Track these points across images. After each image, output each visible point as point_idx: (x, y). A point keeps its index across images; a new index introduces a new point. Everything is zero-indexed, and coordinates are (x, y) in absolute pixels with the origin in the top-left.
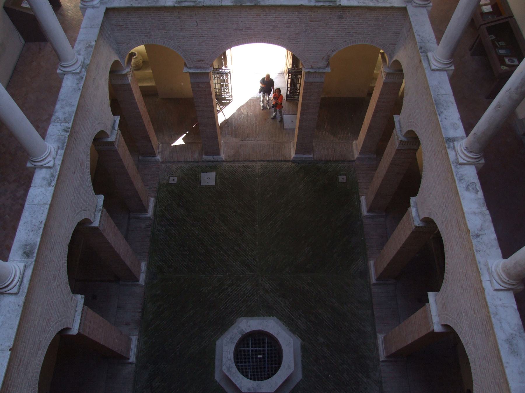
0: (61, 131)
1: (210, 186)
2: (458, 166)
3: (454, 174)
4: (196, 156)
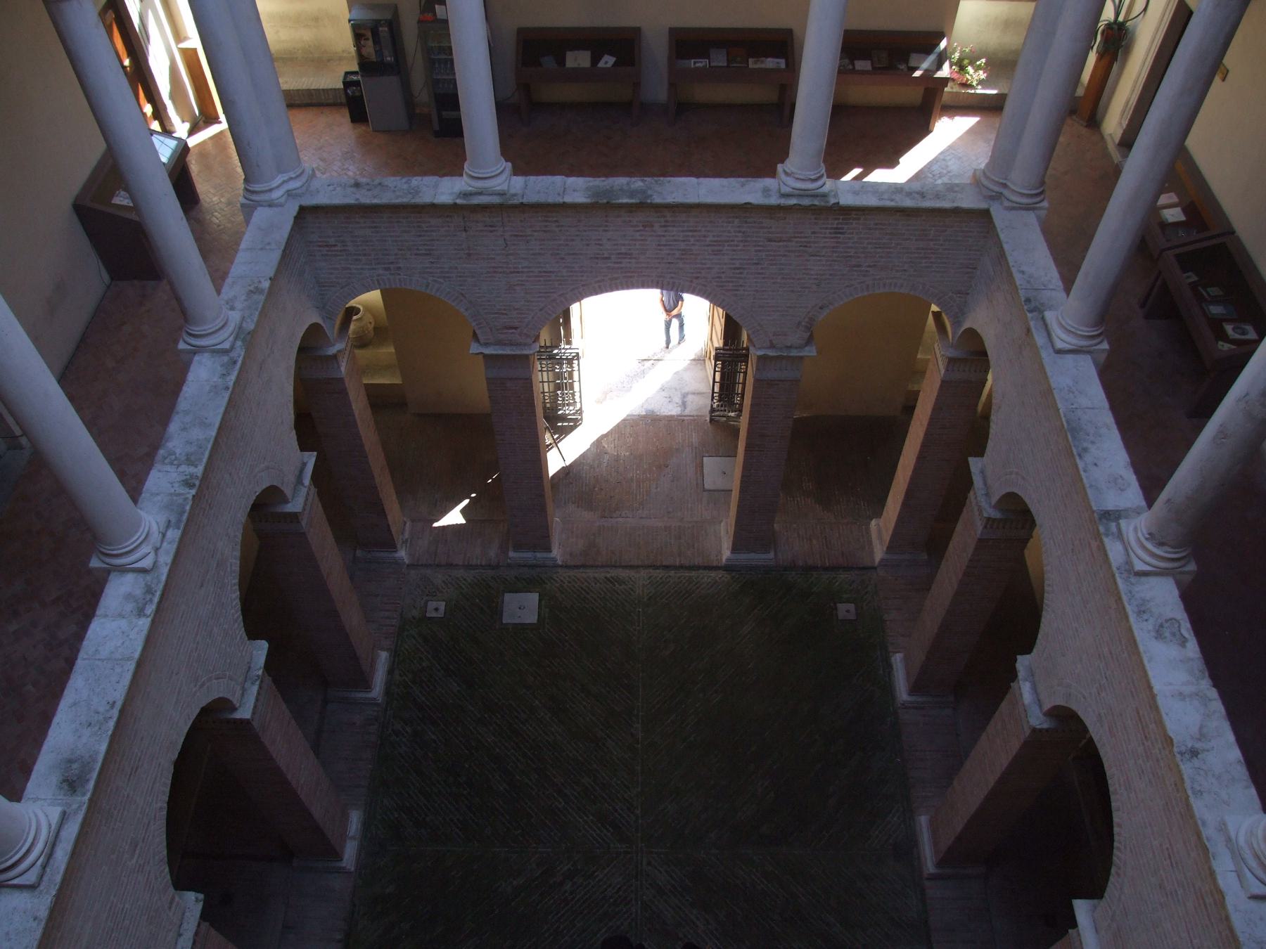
0: (176, 485)
1: (521, 628)
2: (1133, 580)
3: (1124, 598)
4: (493, 553)
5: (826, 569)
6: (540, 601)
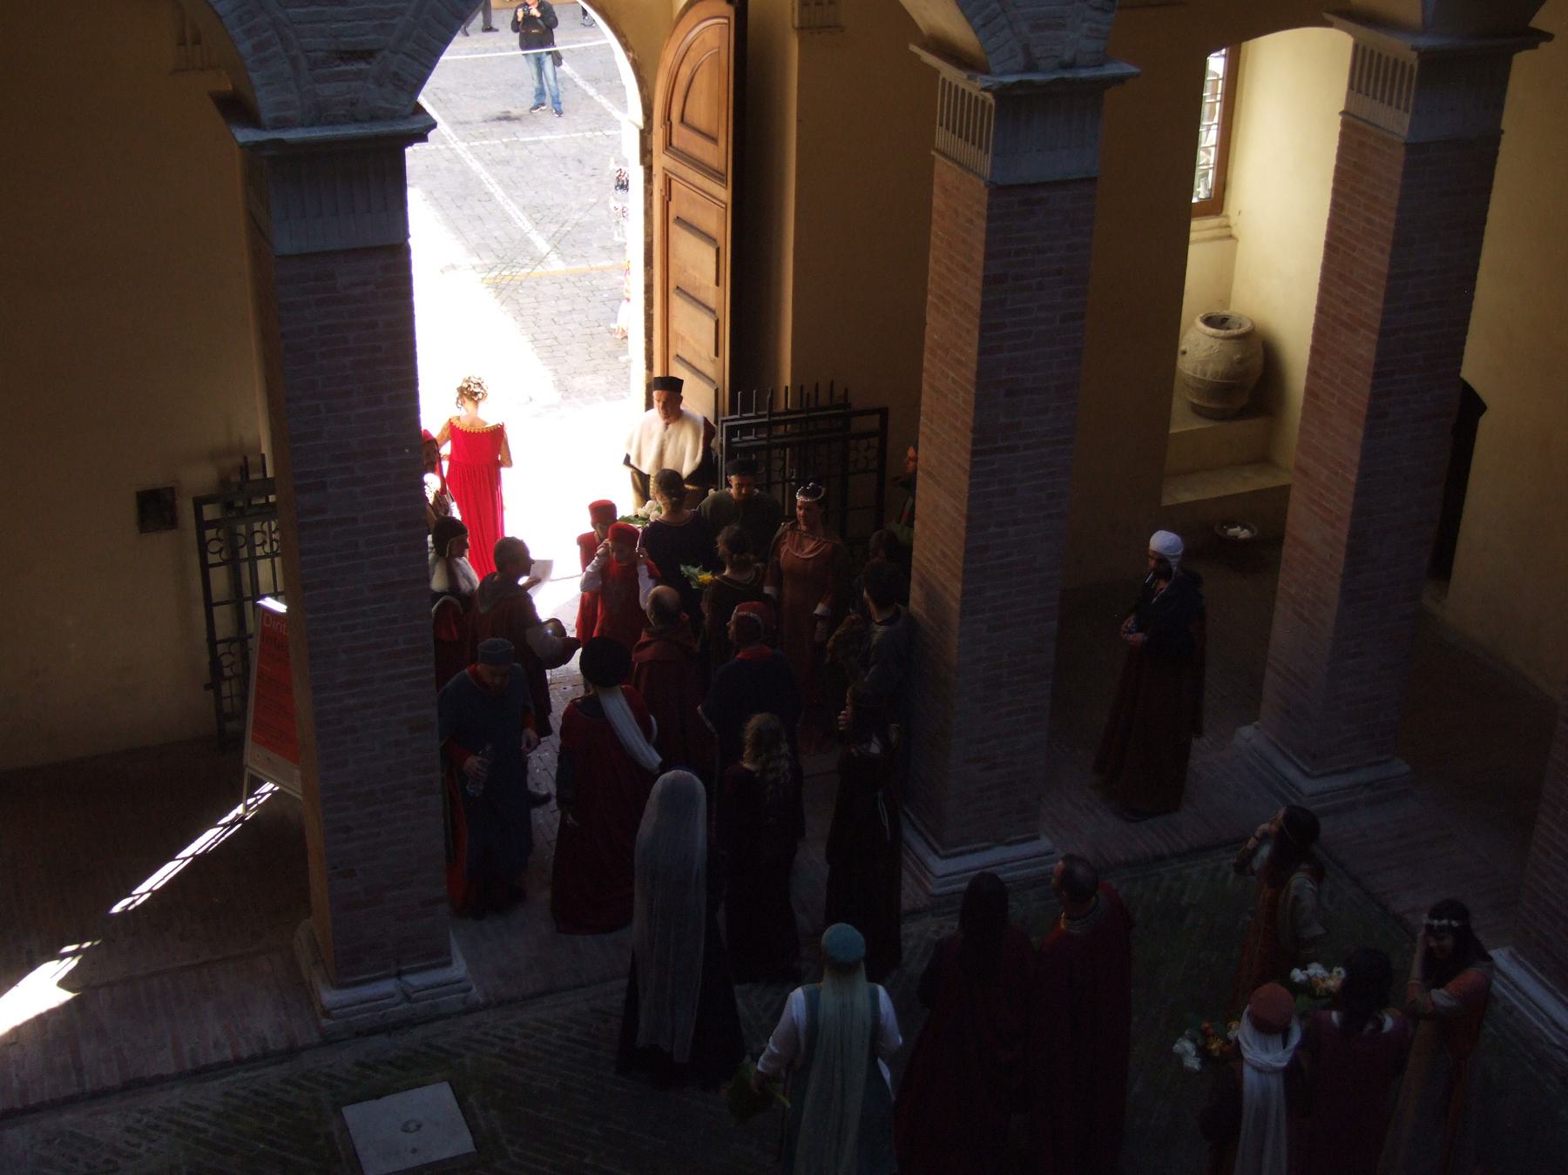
4: (265, 1023)
6: (461, 1099)
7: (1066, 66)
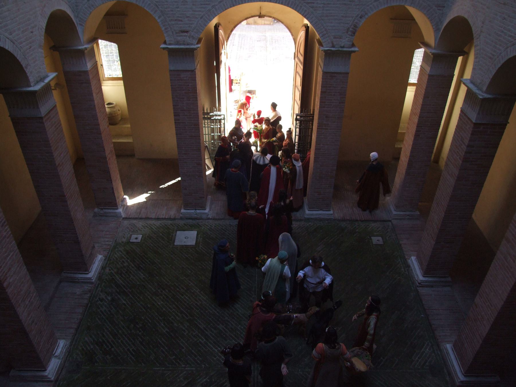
4: (172, 213)
5: (362, 221)
6: (197, 235)
7: (341, 47)
